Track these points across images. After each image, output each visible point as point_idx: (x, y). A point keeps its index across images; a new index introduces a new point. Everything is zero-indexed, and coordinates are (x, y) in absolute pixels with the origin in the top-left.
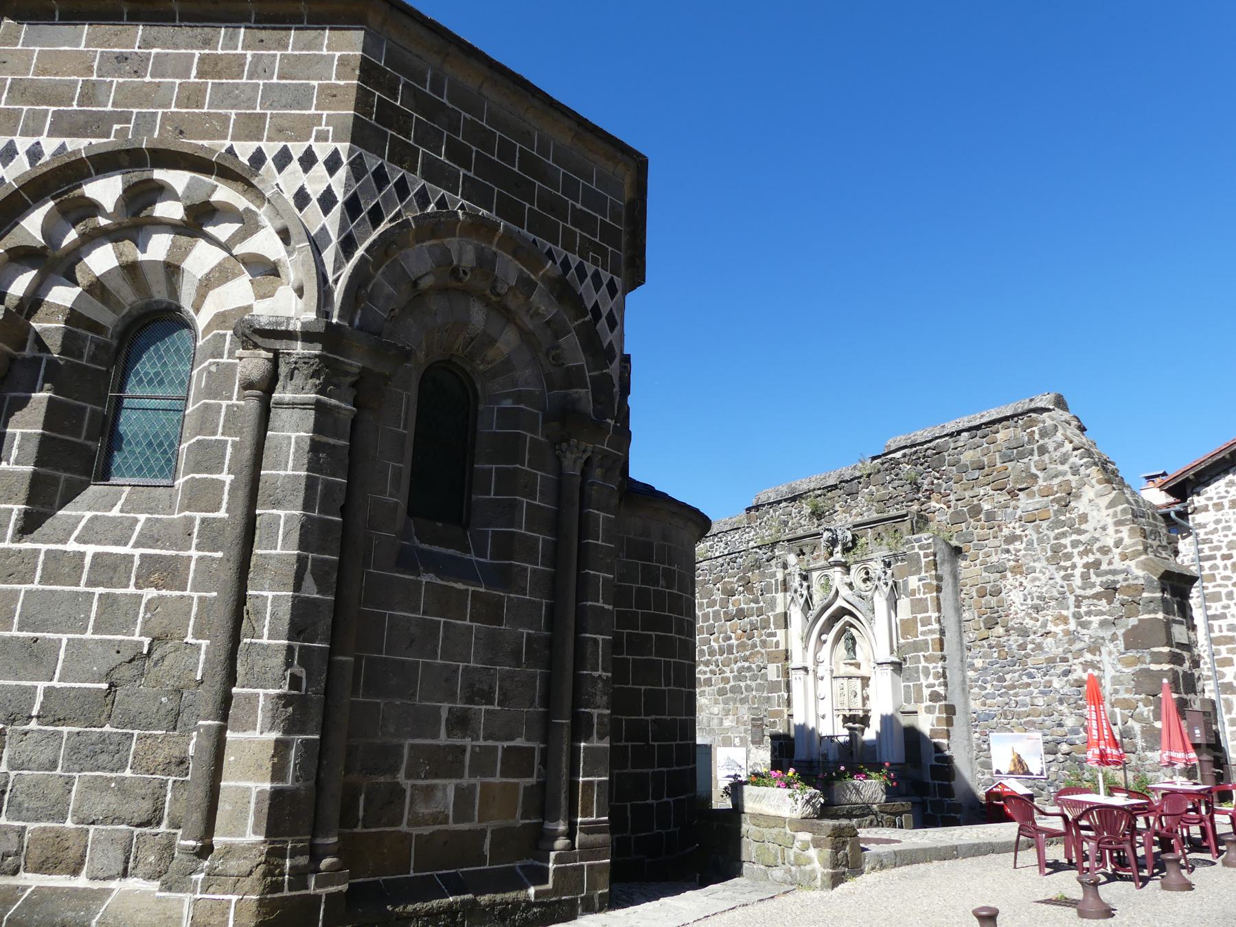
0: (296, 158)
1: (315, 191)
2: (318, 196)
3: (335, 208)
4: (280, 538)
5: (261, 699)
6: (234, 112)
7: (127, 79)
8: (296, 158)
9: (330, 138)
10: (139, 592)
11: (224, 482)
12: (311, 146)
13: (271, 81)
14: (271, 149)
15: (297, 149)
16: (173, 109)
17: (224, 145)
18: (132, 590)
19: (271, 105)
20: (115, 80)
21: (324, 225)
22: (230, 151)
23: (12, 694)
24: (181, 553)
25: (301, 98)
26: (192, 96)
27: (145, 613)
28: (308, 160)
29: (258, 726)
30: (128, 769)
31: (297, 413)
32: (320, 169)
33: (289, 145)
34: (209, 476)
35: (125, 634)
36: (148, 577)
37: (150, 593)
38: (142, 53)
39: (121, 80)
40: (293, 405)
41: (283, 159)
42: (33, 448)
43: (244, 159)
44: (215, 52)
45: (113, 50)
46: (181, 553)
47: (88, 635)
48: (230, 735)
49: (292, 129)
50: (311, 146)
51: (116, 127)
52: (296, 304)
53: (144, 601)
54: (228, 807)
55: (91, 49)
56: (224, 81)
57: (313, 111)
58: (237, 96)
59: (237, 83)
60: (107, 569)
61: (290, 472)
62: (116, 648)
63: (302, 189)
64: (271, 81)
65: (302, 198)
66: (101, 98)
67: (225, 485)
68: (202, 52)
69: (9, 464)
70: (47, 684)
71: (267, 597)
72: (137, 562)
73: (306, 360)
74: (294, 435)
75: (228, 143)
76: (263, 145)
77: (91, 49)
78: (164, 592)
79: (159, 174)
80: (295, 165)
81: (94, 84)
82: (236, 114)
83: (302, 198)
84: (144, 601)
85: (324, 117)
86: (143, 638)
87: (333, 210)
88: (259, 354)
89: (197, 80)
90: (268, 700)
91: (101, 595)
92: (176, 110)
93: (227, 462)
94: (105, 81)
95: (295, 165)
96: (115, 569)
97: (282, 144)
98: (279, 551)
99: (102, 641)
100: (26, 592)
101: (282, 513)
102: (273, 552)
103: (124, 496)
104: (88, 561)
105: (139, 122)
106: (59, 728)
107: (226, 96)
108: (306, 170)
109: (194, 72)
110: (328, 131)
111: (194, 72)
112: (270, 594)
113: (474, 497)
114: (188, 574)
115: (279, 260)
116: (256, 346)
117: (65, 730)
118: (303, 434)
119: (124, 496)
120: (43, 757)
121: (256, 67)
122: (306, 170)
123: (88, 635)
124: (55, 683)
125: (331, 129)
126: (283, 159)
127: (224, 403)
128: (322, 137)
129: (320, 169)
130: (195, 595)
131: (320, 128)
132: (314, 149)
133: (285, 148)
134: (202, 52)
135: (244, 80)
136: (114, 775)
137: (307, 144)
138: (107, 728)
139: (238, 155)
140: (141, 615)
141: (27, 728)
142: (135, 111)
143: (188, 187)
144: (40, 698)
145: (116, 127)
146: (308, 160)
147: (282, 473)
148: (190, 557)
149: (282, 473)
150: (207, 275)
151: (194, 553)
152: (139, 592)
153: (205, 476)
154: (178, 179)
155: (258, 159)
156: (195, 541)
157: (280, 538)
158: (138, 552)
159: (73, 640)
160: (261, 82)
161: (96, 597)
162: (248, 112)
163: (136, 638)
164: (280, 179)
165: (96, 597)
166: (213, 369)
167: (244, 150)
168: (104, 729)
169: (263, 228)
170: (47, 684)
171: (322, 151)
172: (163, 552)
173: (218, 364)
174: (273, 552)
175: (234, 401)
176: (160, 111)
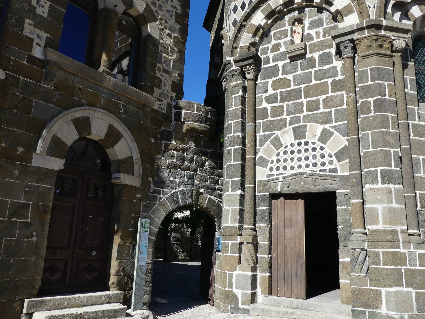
69: (408, 90)
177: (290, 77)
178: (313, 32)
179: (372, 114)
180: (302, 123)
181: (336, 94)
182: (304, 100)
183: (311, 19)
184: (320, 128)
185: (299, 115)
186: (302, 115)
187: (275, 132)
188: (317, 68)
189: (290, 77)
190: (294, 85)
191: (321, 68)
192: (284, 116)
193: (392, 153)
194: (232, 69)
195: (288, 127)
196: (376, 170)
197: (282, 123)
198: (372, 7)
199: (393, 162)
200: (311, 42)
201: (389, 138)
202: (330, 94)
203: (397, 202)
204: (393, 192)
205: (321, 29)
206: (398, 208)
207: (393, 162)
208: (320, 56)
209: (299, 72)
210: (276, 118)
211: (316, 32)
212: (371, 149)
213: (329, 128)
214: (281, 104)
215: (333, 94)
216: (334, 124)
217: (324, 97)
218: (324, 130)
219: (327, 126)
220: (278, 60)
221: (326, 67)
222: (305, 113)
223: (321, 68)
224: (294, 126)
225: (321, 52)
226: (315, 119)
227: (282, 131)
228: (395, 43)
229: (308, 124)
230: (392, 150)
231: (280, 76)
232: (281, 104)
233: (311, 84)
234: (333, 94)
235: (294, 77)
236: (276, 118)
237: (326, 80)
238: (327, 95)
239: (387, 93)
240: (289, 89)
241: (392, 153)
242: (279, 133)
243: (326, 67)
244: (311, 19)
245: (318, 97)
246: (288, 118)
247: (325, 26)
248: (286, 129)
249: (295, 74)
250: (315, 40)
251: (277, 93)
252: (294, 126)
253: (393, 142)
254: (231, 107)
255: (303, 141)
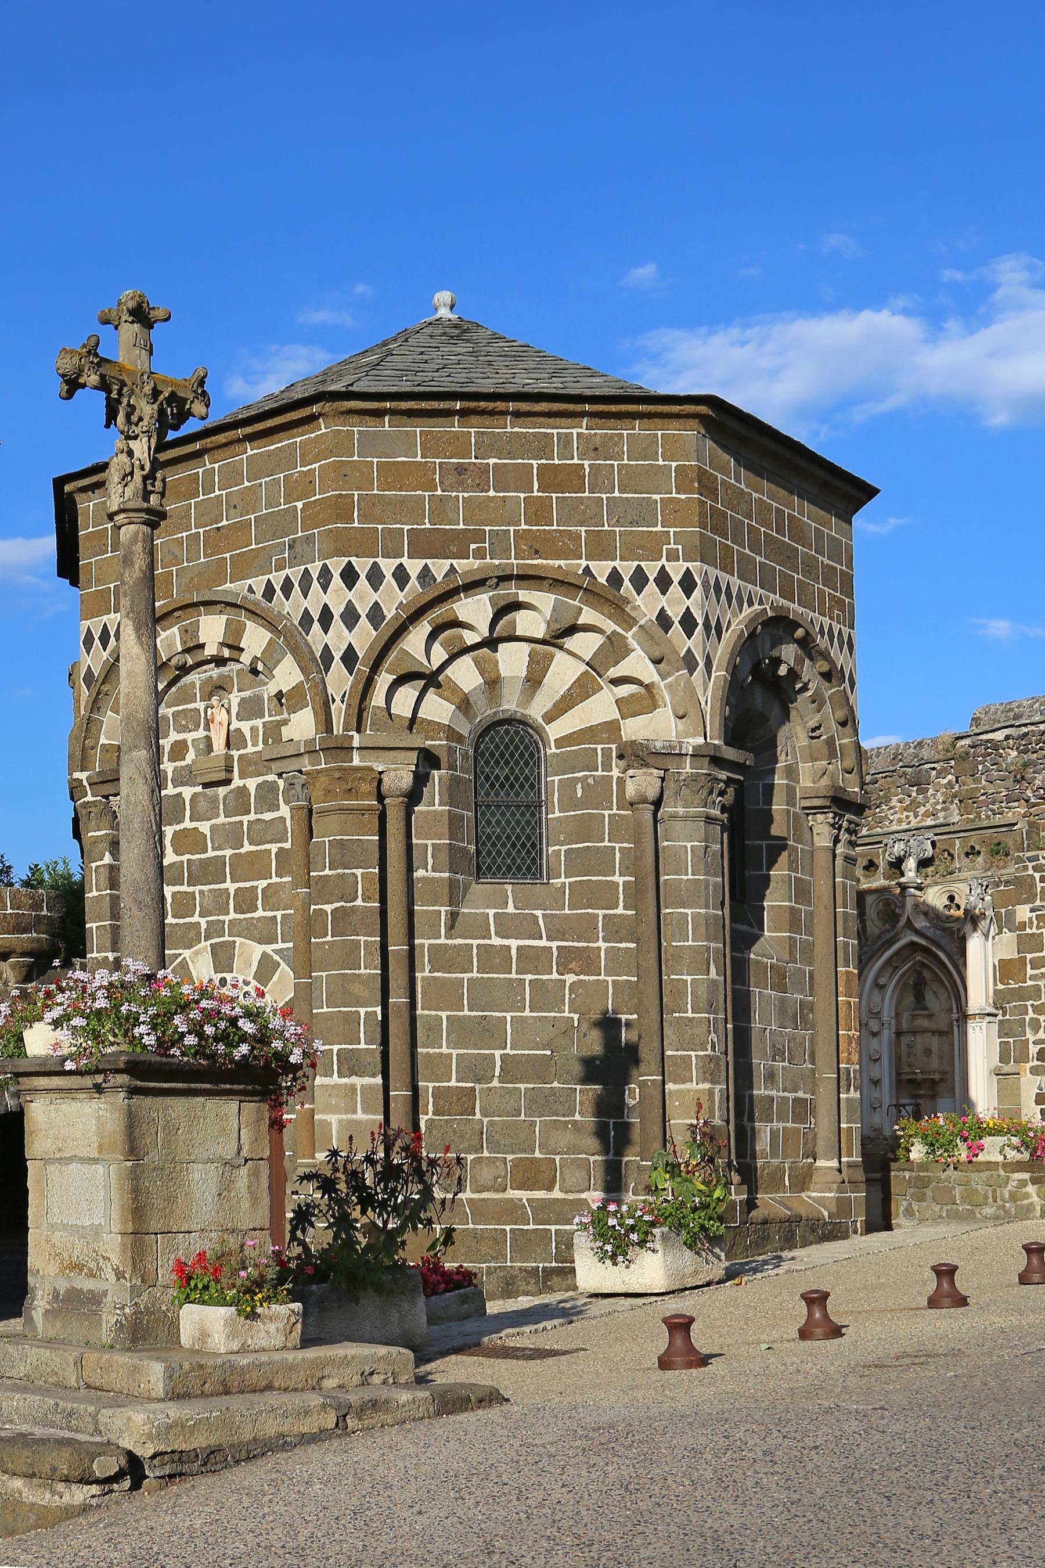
0: (651, 579)
1: (675, 614)
2: (679, 619)
3: (697, 630)
4: (690, 932)
5: (694, 1059)
6: (583, 529)
7: (471, 494)
8: (651, 579)
9: (681, 557)
10: (562, 977)
11: (618, 883)
12: (663, 566)
13: (613, 495)
14: (627, 569)
15: (652, 570)
16: (524, 527)
17: (581, 565)
18: (555, 976)
19: (618, 521)
20: (461, 495)
21: (689, 648)
22: (587, 570)
23: (476, 1060)
24: (591, 945)
25: (644, 513)
26: (538, 512)
27: (570, 995)
28: (664, 581)
29: (694, 1079)
30: (577, 1114)
31: (690, 825)
32: (675, 589)
33: (643, 564)
34: (604, 878)
35: (557, 1012)
36: (567, 966)
37: (570, 978)
38: (480, 463)
39: (466, 495)
40: (686, 818)
41: (639, 580)
42: (444, 857)
43: (602, 580)
44: (552, 462)
45: (450, 460)
46: (591, 945)
47: (527, 1013)
48: (670, 1086)
49: (642, 547)
50: (663, 566)
51: (473, 546)
52: (676, 726)
53: (567, 985)
54: (680, 1138)
55: (428, 460)
56: (567, 495)
57: (659, 528)
58: (584, 512)
59: (581, 497)
60: (531, 959)
61: (690, 877)
62: (552, 1023)
63: (662, 610)
64: (613, 495)
65: (664, 621)
66: (451, 515)
67: (619, 886)
68: (539, 462)
70: (503, 1052)
71: (687, 980)
72: (555, 953)
73: (694, 778)
74: (689, 845)
75: (584, 563)
76: (617, 563)
77: (428, 460)
78: (582, 977)
79: (523, 595)
80: (651, 587)
81: (441, 499)
82: (585, 531)
83: (664, 621)
84: (567, 985)
85: (672, 534)
86: (572, 1015)
87: (695, 633)
88: (651, 773)
89: (540, 494)
90: (699, 1060)
91: (530, 981)
92: (527, 527)
93: (617, 866)
94: (451, 496)
95: (651, 587)
96: (538, 959)
97: (636, 563)
98: (690, 943)
99: (540, 1018)
100: (468, 979)
101: (689, 911)
102: (686, 944)
103: (509, 893)
104: (514, 952)
105: (493, 541)
106: (517, 1085)
107: (572, 512)
108: (664, 593)
109: (536, 486)
110: (678, 549)
111: (536, 486)
112: (689, 978)
113: (747, 873)
114: (600, 962)
115: (653, 683)
116: (647, 766)
117: (522, 1086)
118: (696, 843)
119: (509, 893)
120: (508, 1107)
121: (596, 479)
122: (664, 593)
123: (527, 1013)
124: (508, 1051)
125: (680, 547)
126: (639, 580)
127: (606, 813)
128: (672, 556)
129: (675, 589)
130: (610, 979)
131: (669, 546)
132: (667, 569)
133: (639, 566)
134: (539, 462)
135: (587, 494)
136: (567, 1119)
137: (660, 564)
138: (555, 1084)
139: (596, 575)
140: (567, 996)
141: (491, 1085)
142: (487, 528)
143: (554, 610)
144: (498, 1063)
145: (473, 546)
146: (664, 581)
147: (684, 877)
148: (599, 948)
149: (684, 877)
150: (569, 690)
151: (601, 944)
152: (562, 977)
153: (600, 878)
154: (545, 601)
155: (615, 578)
156: (601, 935)
157: (690, 932)
158: (554, 944)
159: (516, 1017)
160: (604, 496)
161: (527, 982)
162: (596, 529)
163: (566, 1014)
164: (639, 600)
165: (527, 982)
166: (591, 781)
167: (601, 570)
168: (552, 1085)
169: (633, 651)
170: (503, 1052)
171: (676, 571)
172: (576, 944)
173: (594, 776)
174: (686, 944)
175: (615, 811)
176: (512, 529)
177: (205, 827)
178: (245, 727)
179: (329, 938)
180: (226, 938)
181: (284, 880)
182: (231, 886)
183: (243, 694)
184: (257, 950)
185: (221, 918)
186: (227, 918)
187: (181, 951)
188: (252, 816)
189: (205, 827)
190: (214, 849)
191: (259, 816)
192: (196, 918)
193: (362, 1017)
194: (86, 799)
195: (203, 944)
196: (332, 1050)
197: (192, 934)
198: (338, 699)
199: (362, 1035)
200: (242, 752)
201: (357, 988)
202: (275, 879)
203: (365, 1111)
204: (359, 1092)
205: (259, 723)
206: (367, 1121)
207: (362, 1035)
208: (259, 787)
209: (222, 819)
210: (181, 921)
211: (252, 729)
212: (325, 1010)
213: (272, 953)
214: (191, 889)
215: (278, 880)
216: (280, 945)
217: (262, 884)
218: (265, 956)
219: (269, 948)
220: (183, 784)
221: (268, 816)
222: (232, 915)
223: (259, 816)
224: (213, 941)
225: (260, 779)
226: (248, 930)
227: (193, 950)
228: (385, 778)
229: (238, 940)
230: (362, 1011)
231: (187, 824)
232: (191, 889)
233: (242, 851)
234: (278, 880)
235: (213, 828)
236: (181, 921)
237: (267, 846)
238: (269, 881)
239: (360, 893)
240: (203, 856)
241: (362, 1017)
242: (187, 953)
243: (268, 816)
244: (243, 694)
245: (255, 883)
246: (203, 922)
247: (267, 719)
248: (199, 946)
249: (214, 821)
250: (250, 749)
251: (182, 862)
252: (213, 941)
253: (365, 994)
254: (91, 891)
255: (228, 976)
